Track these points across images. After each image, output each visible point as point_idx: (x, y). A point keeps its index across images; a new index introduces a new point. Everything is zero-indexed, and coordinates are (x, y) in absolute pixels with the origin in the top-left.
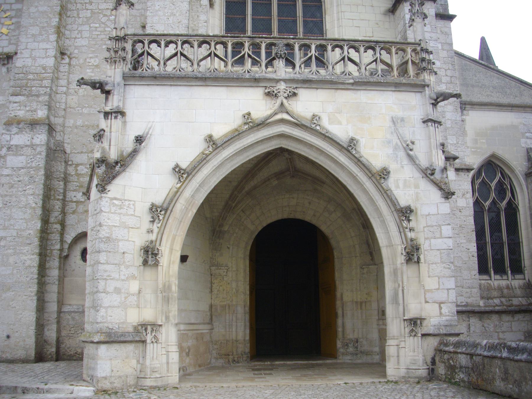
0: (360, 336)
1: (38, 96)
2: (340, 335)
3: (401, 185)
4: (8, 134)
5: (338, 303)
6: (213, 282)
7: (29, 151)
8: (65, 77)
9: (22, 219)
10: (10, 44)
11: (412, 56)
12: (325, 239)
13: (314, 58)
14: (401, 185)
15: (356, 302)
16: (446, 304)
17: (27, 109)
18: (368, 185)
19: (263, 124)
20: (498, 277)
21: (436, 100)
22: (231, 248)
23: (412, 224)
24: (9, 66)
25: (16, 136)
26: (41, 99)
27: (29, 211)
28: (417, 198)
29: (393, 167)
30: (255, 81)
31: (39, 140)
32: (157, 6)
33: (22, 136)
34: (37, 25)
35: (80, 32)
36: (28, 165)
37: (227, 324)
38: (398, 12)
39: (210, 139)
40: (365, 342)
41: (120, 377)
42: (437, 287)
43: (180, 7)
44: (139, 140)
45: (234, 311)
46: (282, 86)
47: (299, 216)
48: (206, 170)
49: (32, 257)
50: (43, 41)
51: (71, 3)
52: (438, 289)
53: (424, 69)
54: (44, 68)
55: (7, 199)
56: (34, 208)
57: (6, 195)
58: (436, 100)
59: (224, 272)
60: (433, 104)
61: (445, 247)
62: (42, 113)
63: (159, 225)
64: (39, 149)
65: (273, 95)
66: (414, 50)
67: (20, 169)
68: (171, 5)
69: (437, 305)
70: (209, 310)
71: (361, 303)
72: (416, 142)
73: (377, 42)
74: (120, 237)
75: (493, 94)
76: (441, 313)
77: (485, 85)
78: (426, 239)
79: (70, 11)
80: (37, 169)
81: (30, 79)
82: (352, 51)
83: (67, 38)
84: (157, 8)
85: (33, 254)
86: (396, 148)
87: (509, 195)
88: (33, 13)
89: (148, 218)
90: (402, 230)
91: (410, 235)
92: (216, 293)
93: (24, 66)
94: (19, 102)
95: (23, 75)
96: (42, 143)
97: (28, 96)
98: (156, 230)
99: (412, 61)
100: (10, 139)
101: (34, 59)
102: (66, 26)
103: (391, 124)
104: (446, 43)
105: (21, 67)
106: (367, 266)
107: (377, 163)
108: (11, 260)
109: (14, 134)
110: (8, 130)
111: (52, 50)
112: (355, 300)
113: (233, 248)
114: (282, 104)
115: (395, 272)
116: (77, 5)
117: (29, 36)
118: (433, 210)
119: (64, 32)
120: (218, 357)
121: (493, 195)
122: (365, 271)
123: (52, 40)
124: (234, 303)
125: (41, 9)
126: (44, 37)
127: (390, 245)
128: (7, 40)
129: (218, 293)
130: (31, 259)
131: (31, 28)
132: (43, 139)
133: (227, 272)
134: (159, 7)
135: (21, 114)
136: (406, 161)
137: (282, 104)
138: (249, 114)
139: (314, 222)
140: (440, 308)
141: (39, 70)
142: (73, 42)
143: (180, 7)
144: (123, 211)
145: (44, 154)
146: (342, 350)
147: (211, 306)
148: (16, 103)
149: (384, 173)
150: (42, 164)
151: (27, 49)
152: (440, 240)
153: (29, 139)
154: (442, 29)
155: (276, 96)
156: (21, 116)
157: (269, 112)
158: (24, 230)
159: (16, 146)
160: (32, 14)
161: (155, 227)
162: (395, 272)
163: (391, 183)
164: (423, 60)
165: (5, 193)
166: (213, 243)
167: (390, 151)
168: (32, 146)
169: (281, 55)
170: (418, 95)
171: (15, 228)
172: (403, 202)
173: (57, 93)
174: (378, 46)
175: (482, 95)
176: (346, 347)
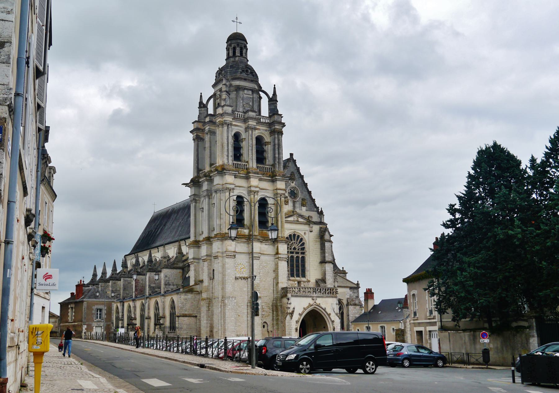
35: (260, 272)
38: (323, 264)
39: (304, 308)
44: (294, 308)
87: (342, 309)
89: (296, 323)
90: (333, 325)
107: (329, 313)
127: (330, 327)
136: (333, 312)
141: (257, 284)
149: (330, 314)
161: (297, 325)
163: (331, 316)
172: (332, 320)
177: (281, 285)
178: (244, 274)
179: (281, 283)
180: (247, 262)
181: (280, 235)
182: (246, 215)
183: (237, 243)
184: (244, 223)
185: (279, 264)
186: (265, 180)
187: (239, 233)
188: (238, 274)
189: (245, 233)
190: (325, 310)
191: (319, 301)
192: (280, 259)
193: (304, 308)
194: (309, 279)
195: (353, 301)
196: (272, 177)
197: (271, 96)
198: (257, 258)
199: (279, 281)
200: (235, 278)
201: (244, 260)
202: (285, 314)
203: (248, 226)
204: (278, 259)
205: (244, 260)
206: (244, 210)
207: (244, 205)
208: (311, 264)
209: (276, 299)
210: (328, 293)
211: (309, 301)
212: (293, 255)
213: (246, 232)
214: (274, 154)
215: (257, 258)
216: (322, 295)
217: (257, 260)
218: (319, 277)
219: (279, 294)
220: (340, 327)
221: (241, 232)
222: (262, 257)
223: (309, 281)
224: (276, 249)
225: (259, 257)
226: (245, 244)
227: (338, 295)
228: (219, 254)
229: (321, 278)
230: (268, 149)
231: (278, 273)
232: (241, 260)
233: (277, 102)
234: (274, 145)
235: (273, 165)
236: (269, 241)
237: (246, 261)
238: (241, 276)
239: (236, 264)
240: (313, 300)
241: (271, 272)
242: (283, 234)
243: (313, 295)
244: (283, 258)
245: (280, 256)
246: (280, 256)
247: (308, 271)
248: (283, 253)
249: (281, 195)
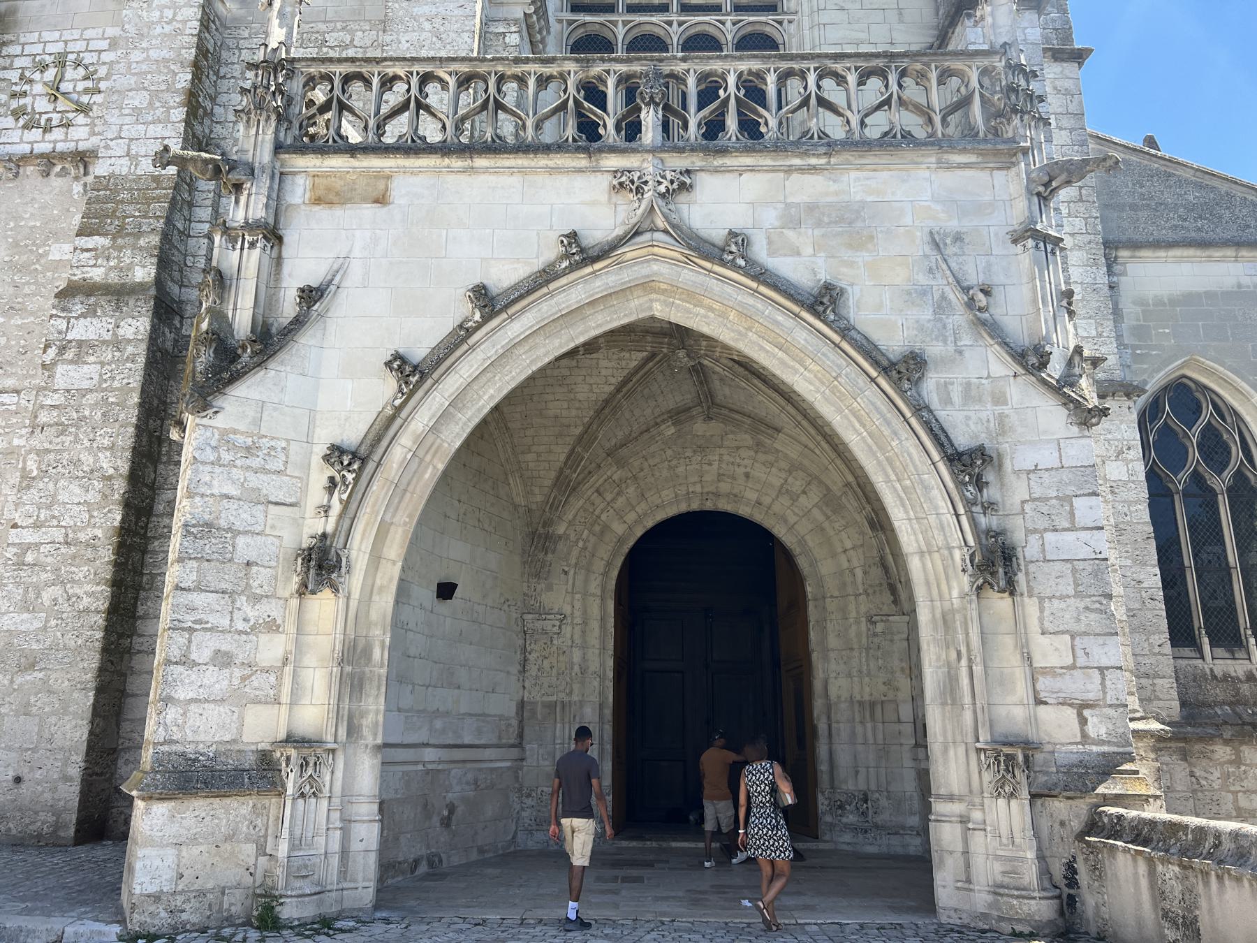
0: (873, 787)
1: (139, 235)
2: (824, 779)
3: (956, 396)
4: (64, 318)
5: (818, 704)
6: (529, 649)
8: (209, 202)
9: (79, 503)
11: (982, 86)
12: (788, 555)
13: (732, 101)
14: (956, 396)
15: (861, 703)
16: (1097, 711)
17: (112, 264)
20: (1220, 652)
21: (1046, 185)
22: (572, 573)
23: (991, 493)
25: (82, 320)
26: (142, 242)
27: (98, 485)
29: (934, 350)
31: (133, 330)
32: (404, 42)
33: (95, 321)
34: (145, 88)
36: (105, 385)
37: (557, 746)
40: (884, 802)
41: (201, 894)
42: (1069, 661)
43: (455, 44)
45: (574, 717)
47: (725, 506)
48: (466, 368)
49: (99, 588)
51: (229, 49)
52: (1073, 667)
56: (110, 478)
57: (48, 451)
58: (1046, 185)
59: (554, 626)
60: (1039, 194)
61: (1085, 553)
63: (345, 497)
65: (631, 190)
67: (84, 393)
68: (434, 39)
69: (1071, 713)
70: (517, 713)
71: (873, 705)
72: (998, 294)
73: (891, 56)
74: (239, 525)
75: (1186, 224)
76: (1084, 735)
77: (1166, 205)
78: (1029, 532)
79: (227, 64)
81: (122, 202)
82: (828, 83)
83: (217, 123)
85: (98, 584)
86: (941, 306)
88: (137, 62)
92: (534, 674)
94: (95, 249)
95: (108, 192)
96: (140, 337)
98: (336, 508)
99: (982, 96)
100: (68, 328)
102: (216, 97)
103: (927, 249)
104: (1068, 113)
105: (104, 177)
106: (884, 618)
108: (47, 596)
109: (76, 318)
110: (63, 310)
111: (175, 140)
112: (858, 697)
113: (575, 573)
115: (946, 621)
116: (240, 53)
117: (126, 111)
118: (1047, 457)
119: (212, 109)
120: (534, 827)
121: (1194, 455)
122: (880, 628)
123: (175, 120)
124: (575, 698)
126: (158, 112)
128: (87, 125)
129: (540, 674)
130: (89, 595)
131: (130, 94)
132: (141, 328)
133: (560, 627)
134: (408, 44)
138: (573, 236)
139: (758, 517)
140: (1083, 721)
142: (230, 130)
143: (455, 44)
144: (256, 462)
145: (142, 360)
146: (828, 819)
147: (522, 705)
148: (87, 250)
151: (121, 138)
152: (1070, 537)
153: (110, 327)
154: (1058, 83)
156: (98, 279)
158: (82, 529)
159: (80, 343)
160: (134, 65)
162: (946, 621)
165: (47, 445)
166: (532, 562)
168: (117, 344)
169: (652, 98)
171: (63, 523)
172: (962, 439)
173: (190, 236)
174: (893, 65)
175: (1158, 226)
176: (840, 812)
205: (88, 34)
212: (656, 18)
232: (67, 35)
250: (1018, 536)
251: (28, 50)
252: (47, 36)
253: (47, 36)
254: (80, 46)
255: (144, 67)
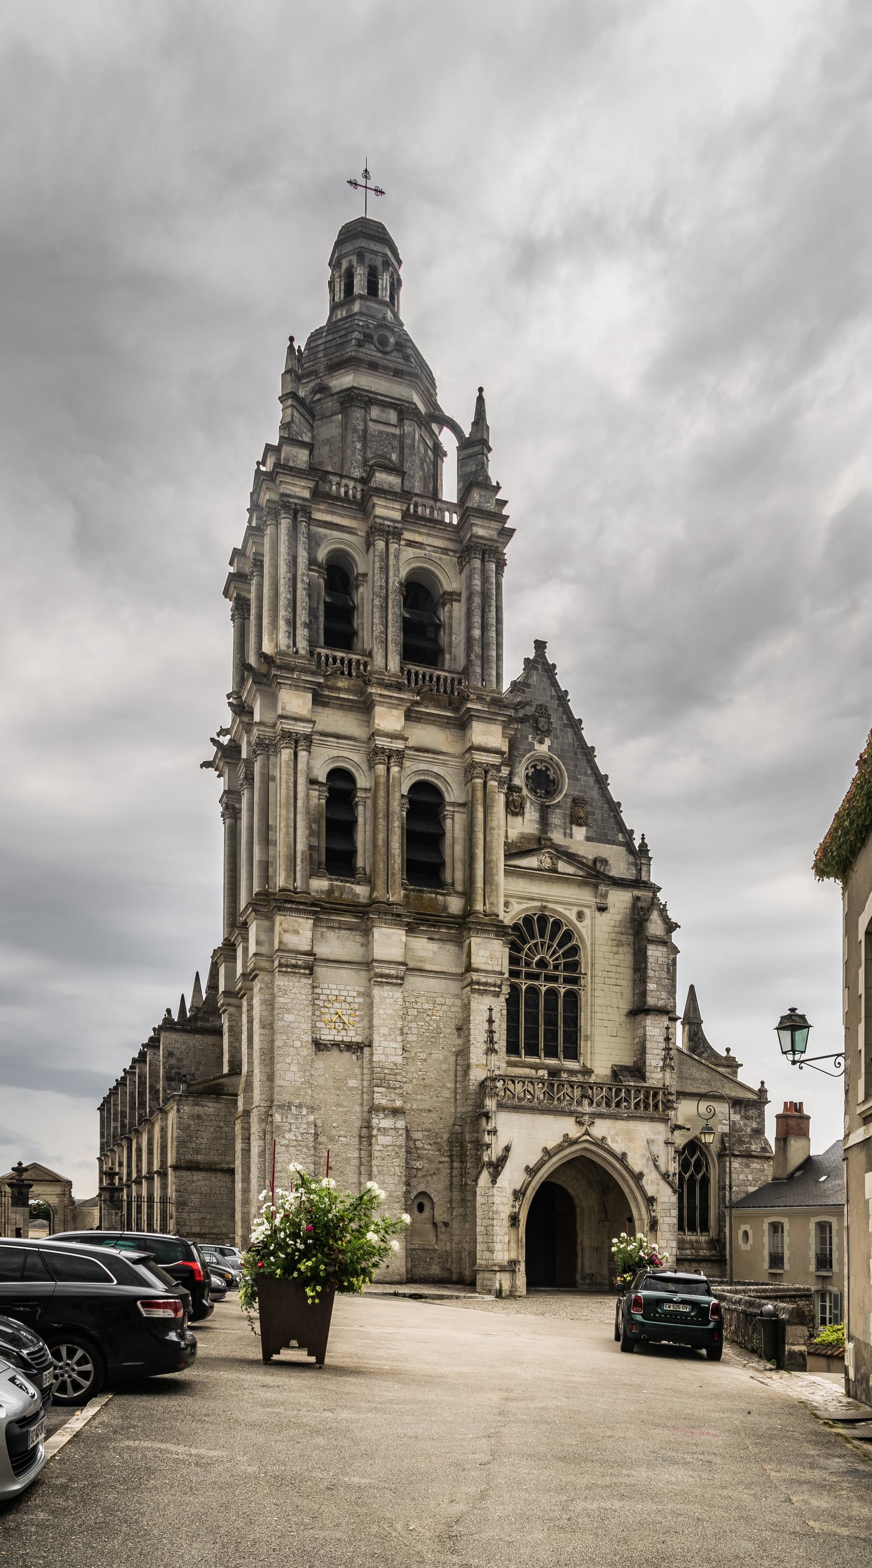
1: (395, 1088)
7: (393, 1133)
10: (357, 1034)
18: (631, 1182)
19: (575, 1142)
23: (654, 1207)
24: (359, 1054)
27: (397, 1178)
28: (658, 1192)
29: (645, 1172)
30: (571, 1114)
46: (587, 1118)
50: (392, 1040)
53: (669, 1108)
54: (395, 1065)
55: (380, 1168)
62: (398, 1103)
64: (400, 1132)
66: (664, 1093)
67: (387, 1146)
80: (400, 1147)
84: (478, 1022)
86: (648, 1160)
90: (649, 1211)
91: (653, 1214)
93: (379, 1062)
97: (388, 1088)
101: (387, 1055)
107: (637, 1169)
114: (587, 1130)
118: (667, 1200)
125: (388, 1011)
127: (641, 1219)
135: (384, 1102)
136: (653, 1168)
137: (587, 1130)
138: (567, 1135)
141: (392, 1066)
145: (404, 1135)
149: (641, 1175)
150: (403, 1143)
155: (583, 1124)
157: (579, 1134)
163: (644, 1182)
164: (669, 1101)
167: (645, 1161)
168: (395, 1129)
170: (663, 1125)
172: (650, 1194)
177: (477, 1075)
178: (352, 1033)
179: (477, 1066)
180: (359, 994)
181: (479, 907)
182: (362, 837)
183: (325, 930)
184: (356, 863)
185: (474, 1005)
186: (434, 720)
187: (337, 894)
188: (326, 1031)
189: (357, 895)
190: (622, 1159)
191: (601, 1129)
192: (477, 987)
193: (545, 1150)
194: (589, 1065)
195: (743, 1142)
196: (456, 709)
197: (467, 431)
198: (394, 981)
199: (471, 1061)
200: (319, 1045)
201: (348, 988)
202: (480, 1166)
203: (368, 871)
204: (469, 988)
205: (348, 988)
206: (356, 821)
207: (357, 804)
208: (598, 1016)
209: (459, 1121)
210: (637, 1105)
211: (567, 1127)
213: (361, 891)
214: (469, 628)
215: (394, 981)
216: (613, 1110)
217: (395, 988)
218: (627, 1060)
219: (469, 1102)
220: (675, 1221)
221: (342, 894)
222: (415, 982)
223: (588, 1072)
224: (464, 956)
225: (402, 978)
226: (353, 933)
227: (672, 1113)
228: (264, 964)
229: (631, 1065)
230: (451, 612)
231: (469, 1034)
232: (339, 987)
233: (490, 449)
234: (470, 599)
235: (466, 672)
236: (440, 927)
237: (357, 988)
238: (338, 1038)
239: (322, 997)
240: (580, 1123)
241: (449, 1030)
242: (492, 904)
243: (580, 1109)
244: (486, 984)
245: (475, 976)
246: (475, 976)
247: (586, 1040)
248: (489, 968)
249: (486, 772)
250: (659, 1218)
251: (325, 991)
252: (331, 986)
253: (331, 986)
254: (345, 993)
255: (385, 1016)
